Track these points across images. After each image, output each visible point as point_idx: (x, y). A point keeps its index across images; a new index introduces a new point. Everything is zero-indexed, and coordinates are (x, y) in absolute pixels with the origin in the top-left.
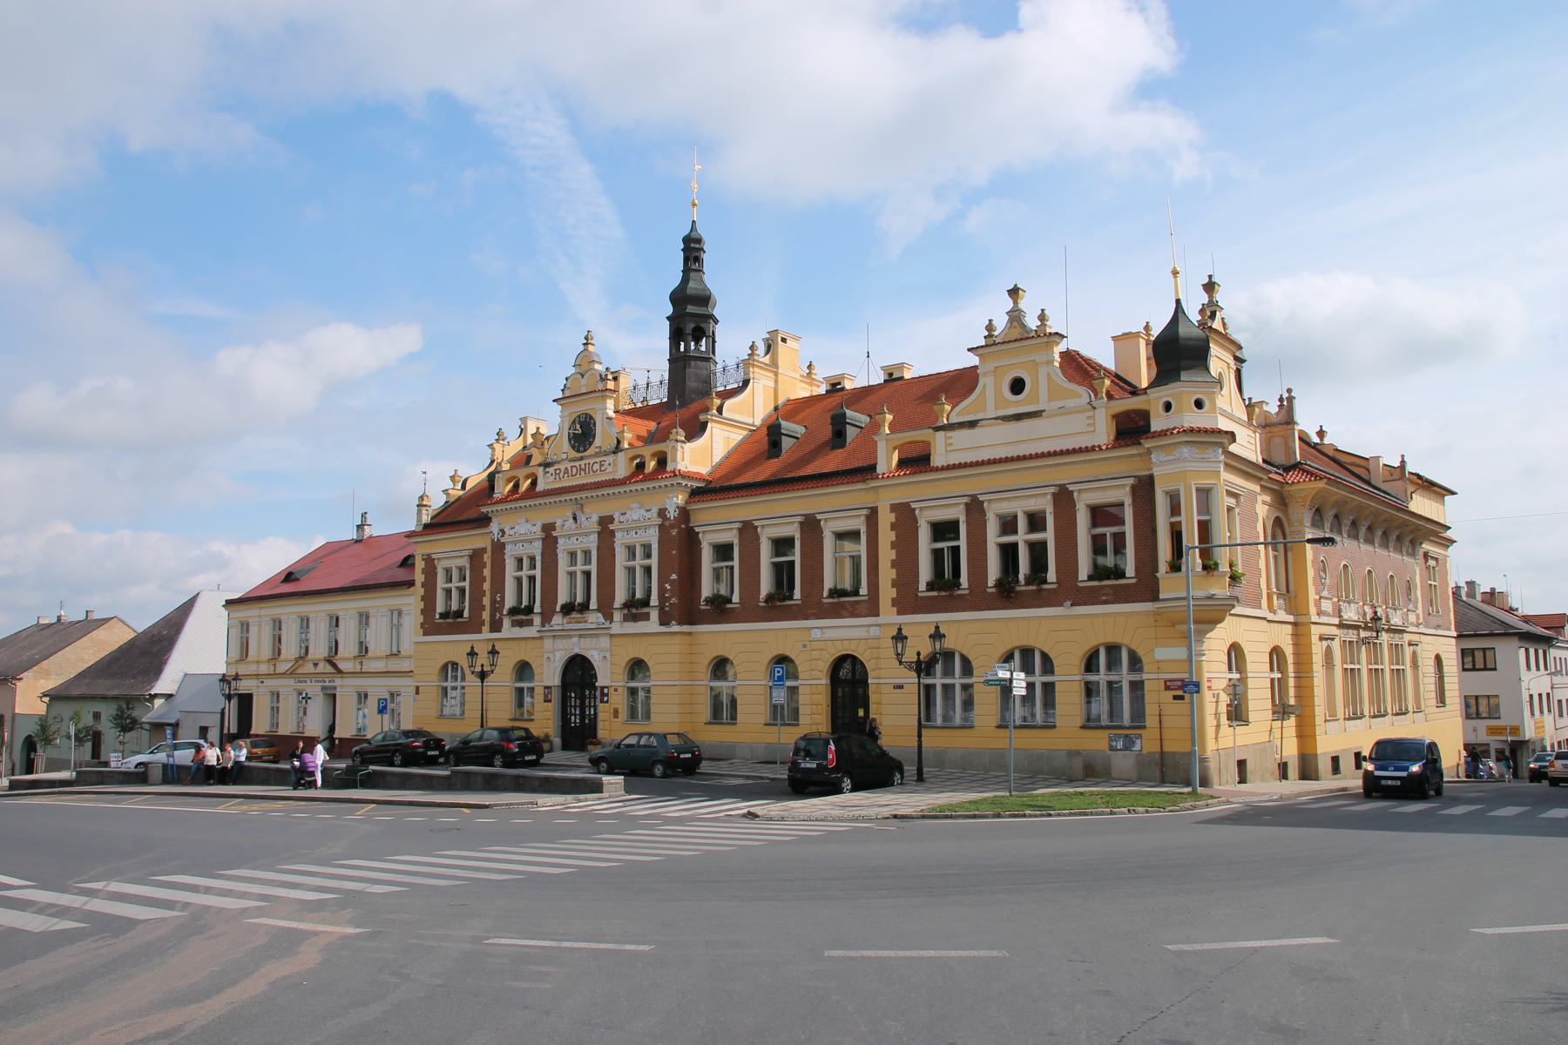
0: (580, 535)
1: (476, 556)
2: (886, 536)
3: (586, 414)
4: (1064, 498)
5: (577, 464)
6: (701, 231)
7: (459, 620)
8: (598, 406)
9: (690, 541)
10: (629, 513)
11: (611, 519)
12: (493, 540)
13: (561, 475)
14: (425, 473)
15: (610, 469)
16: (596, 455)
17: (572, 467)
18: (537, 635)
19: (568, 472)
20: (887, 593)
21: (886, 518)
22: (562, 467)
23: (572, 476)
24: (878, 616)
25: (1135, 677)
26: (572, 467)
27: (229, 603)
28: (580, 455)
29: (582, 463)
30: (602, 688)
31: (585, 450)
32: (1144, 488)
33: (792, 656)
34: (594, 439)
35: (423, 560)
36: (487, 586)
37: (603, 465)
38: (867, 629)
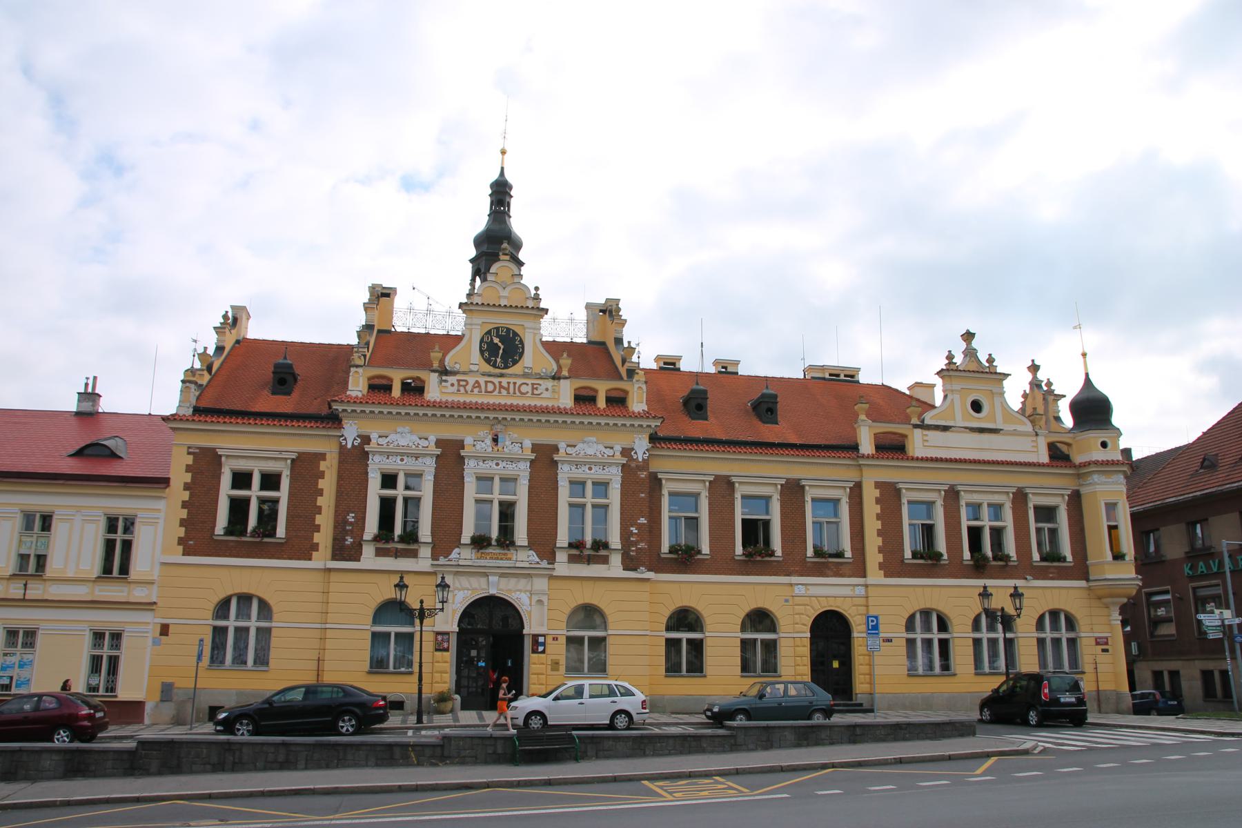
0: (503, 459)
1: (305, 466)
2: (871, 509)
3: (508, 330)
4: (1020, 498)
5: (496, 380)
7: (266, 540)
8: (528, 323)
9: (655, 482)
10: (580, 446)
11: (555, 449)
12: (342, 448)
13: (469, 388)
14: (195, 341)
15: (546, 395)
16: (525, 375)
17: (486, 382)
18: (431, 570)
19: (479, 386)
20: (873, 557)
21: (870, 495)
22: (471, 380)
23: (486, 392)
24: (865, 576)
25: (1072, 635)
26: (486, 382)
28: (498, 371)
29: (504, 381)
30: (535, 637)
31: (506, 367)
32: (1075, 500)
33: (607, 611)
34: (520, 358)
35: (189, 453)
36: (326, 502)
37: (537, 389)
38: (852, 588)
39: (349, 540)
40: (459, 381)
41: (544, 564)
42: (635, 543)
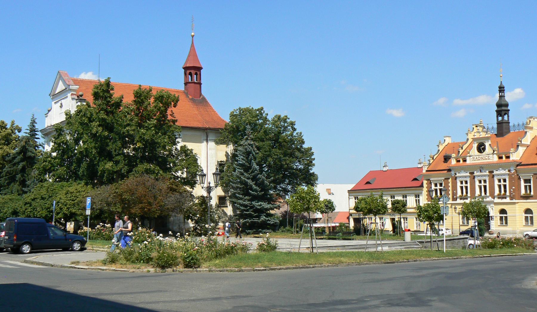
3: (482, 143)
5: (480, 156)
6: (504, 84)
14: (425, 156)
19: (477, 159)
27: (348, 191)
29: (482, 156)
30: (492, 216)
39: (455, 197)
40: (473, 158)
41: (493, 200)
42: (512, 194)
